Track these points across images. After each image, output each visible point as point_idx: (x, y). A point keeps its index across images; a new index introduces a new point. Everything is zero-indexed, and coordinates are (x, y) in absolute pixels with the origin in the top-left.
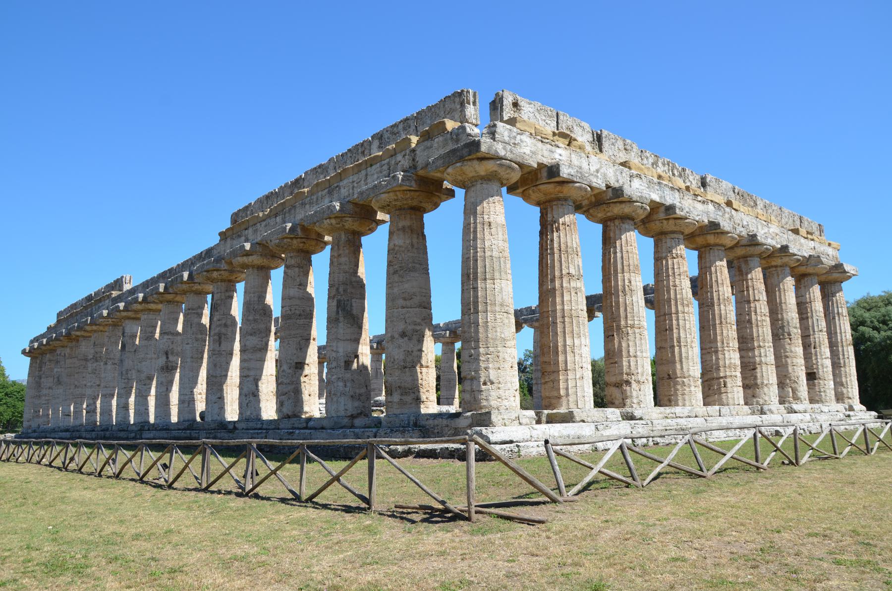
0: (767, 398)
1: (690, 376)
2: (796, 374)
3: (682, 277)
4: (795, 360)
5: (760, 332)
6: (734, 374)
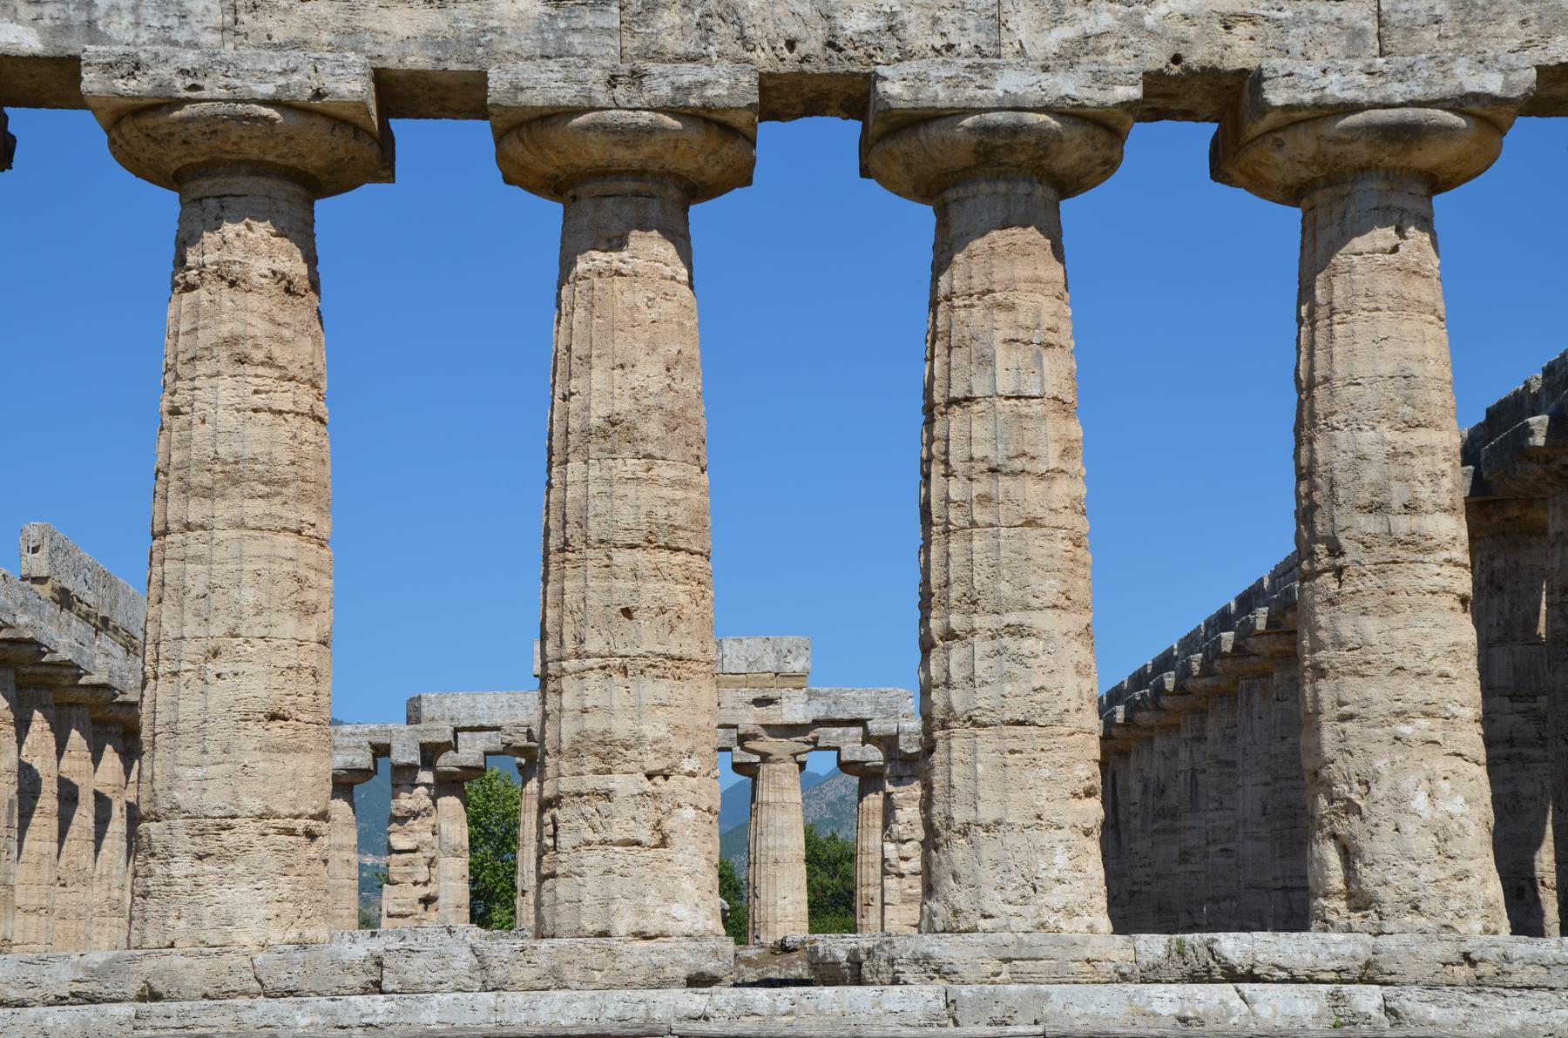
0: (961, 899)
1: (175, 808)
2: (1355, 765)
3: (202, 368)
4: (1353, 689)
5: (957, 559)
6: (592, 782)
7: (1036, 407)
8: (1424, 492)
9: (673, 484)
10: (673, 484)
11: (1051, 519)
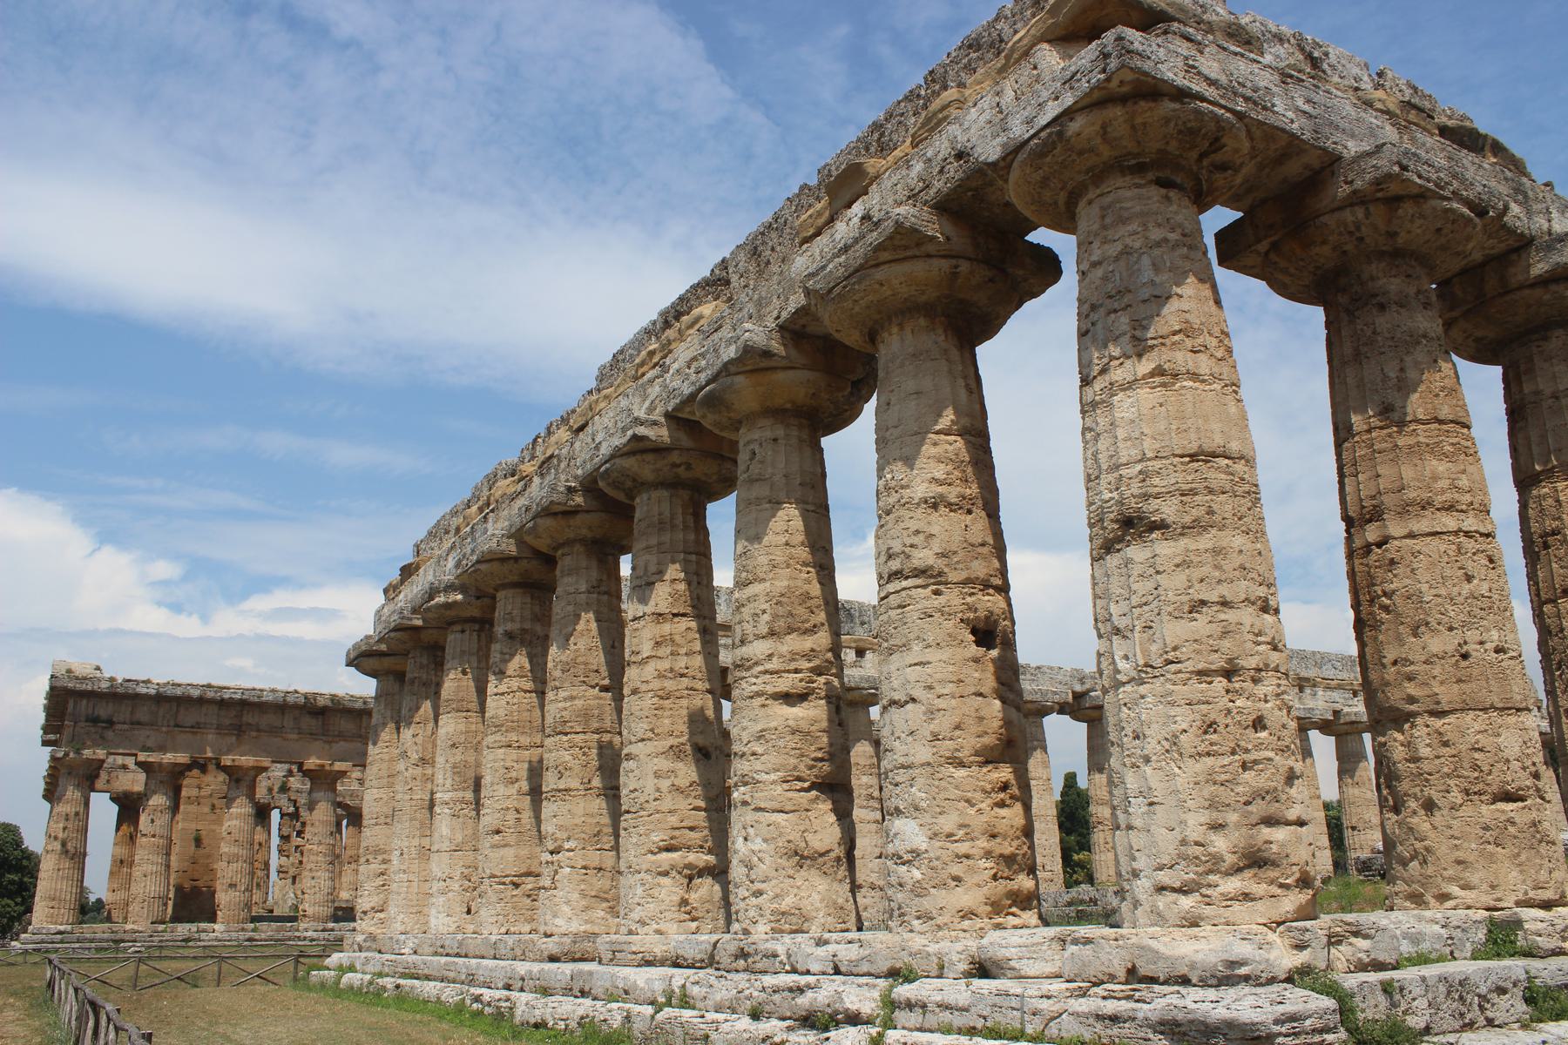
7: (642, 623)
8: (748, 628)
9: (565, 700)
10: (565, 700)
11: (644, 687)
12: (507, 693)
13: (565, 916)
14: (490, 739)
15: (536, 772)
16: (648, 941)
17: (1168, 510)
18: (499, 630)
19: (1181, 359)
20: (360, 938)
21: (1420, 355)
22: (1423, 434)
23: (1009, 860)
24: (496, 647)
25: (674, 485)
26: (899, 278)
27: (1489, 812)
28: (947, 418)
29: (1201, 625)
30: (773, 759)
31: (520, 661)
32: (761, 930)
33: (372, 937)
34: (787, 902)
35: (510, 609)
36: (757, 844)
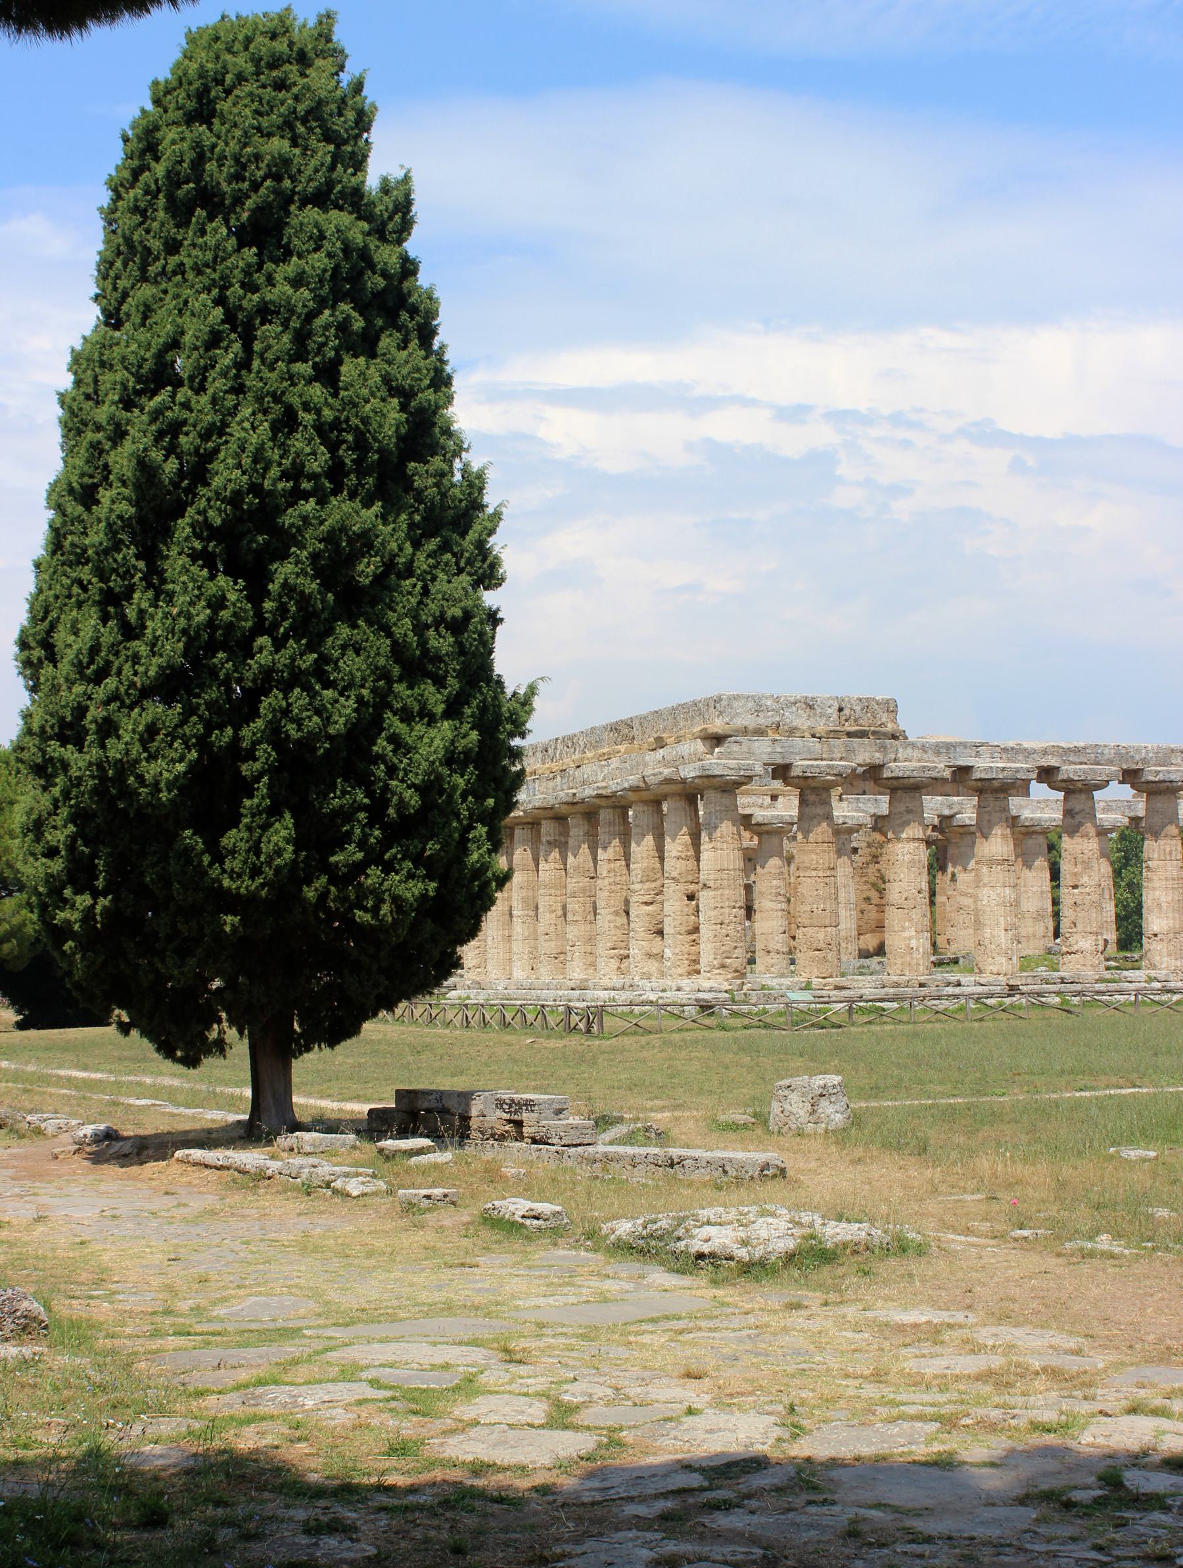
12: (549, 868)
13: (576, 972)
14: (542, 891)
15: (564, 908)
16: (606, 982)
17: (711, 884)
18: (544, 839)
19: (719, 845)
20: (468, 982)
21: (815, 822)
22: (810, 847)
23: (694, 961)
24: (542, 848)
25: (614, 807)
26: (667, 789)
27: (811, 953)
28: (685, 829)
29: (716, 912)
30: (640, 924)
31: (555, 854)
32: (637, 978)
33: (475, 982)
34: (645, 970)
35: (548, 829)
36: (636, 951)
